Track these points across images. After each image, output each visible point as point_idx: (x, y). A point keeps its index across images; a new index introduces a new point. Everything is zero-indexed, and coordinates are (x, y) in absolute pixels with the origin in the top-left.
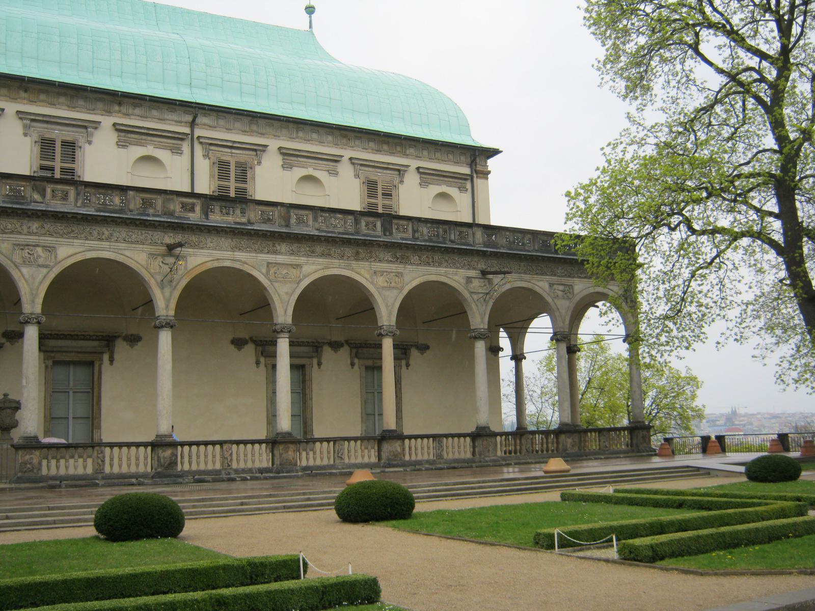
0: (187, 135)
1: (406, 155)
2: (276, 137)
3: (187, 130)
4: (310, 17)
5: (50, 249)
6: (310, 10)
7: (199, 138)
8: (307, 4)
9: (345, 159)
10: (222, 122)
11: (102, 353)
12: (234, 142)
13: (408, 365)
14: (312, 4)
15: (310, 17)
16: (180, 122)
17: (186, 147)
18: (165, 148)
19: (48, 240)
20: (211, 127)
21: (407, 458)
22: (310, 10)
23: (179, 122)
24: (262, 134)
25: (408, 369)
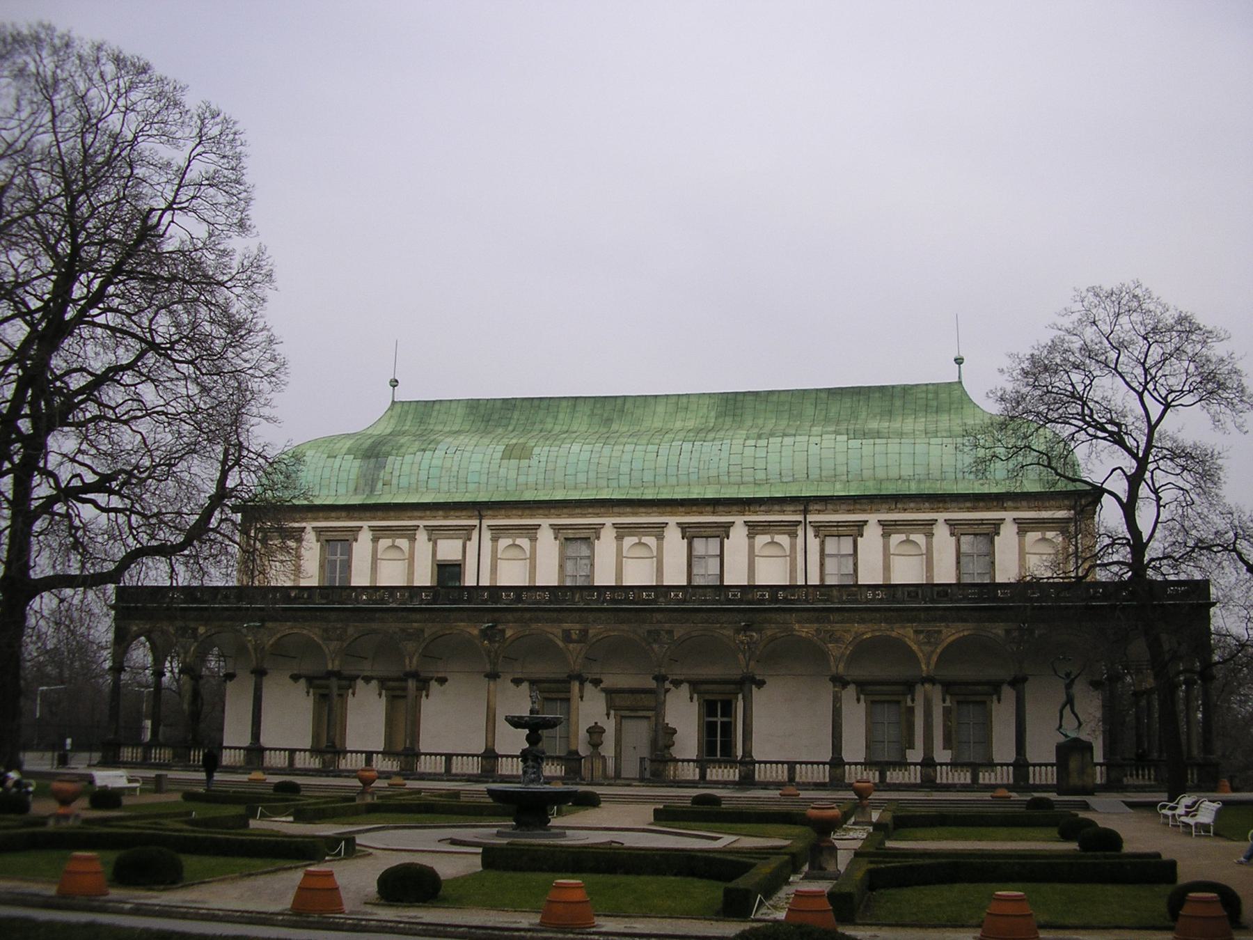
0: (801, 522)
1: (1005, 509)
2: (878, 511)
3: (800, 518)
4: (960, 367)
5: (670, 632)
6: (959, 361)
7: (810, 522)
8: (955, 355)
9: (941, 521)
10: (830, 507)
11: (738, 694)
12: (838, 522)
13: (999, 700)
14: (962, 354)
15: (960, 367)
16: (795, 511)
17: (800, 532)
18: (784, 533)
19: (667, 626)
20: (819, 512)
21: (938, 781)
22: (959, 361)
23: (795, 512)
24: (864, 511)
25: (999, 703)
